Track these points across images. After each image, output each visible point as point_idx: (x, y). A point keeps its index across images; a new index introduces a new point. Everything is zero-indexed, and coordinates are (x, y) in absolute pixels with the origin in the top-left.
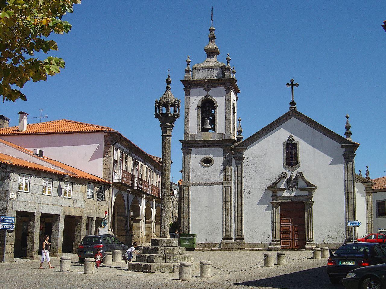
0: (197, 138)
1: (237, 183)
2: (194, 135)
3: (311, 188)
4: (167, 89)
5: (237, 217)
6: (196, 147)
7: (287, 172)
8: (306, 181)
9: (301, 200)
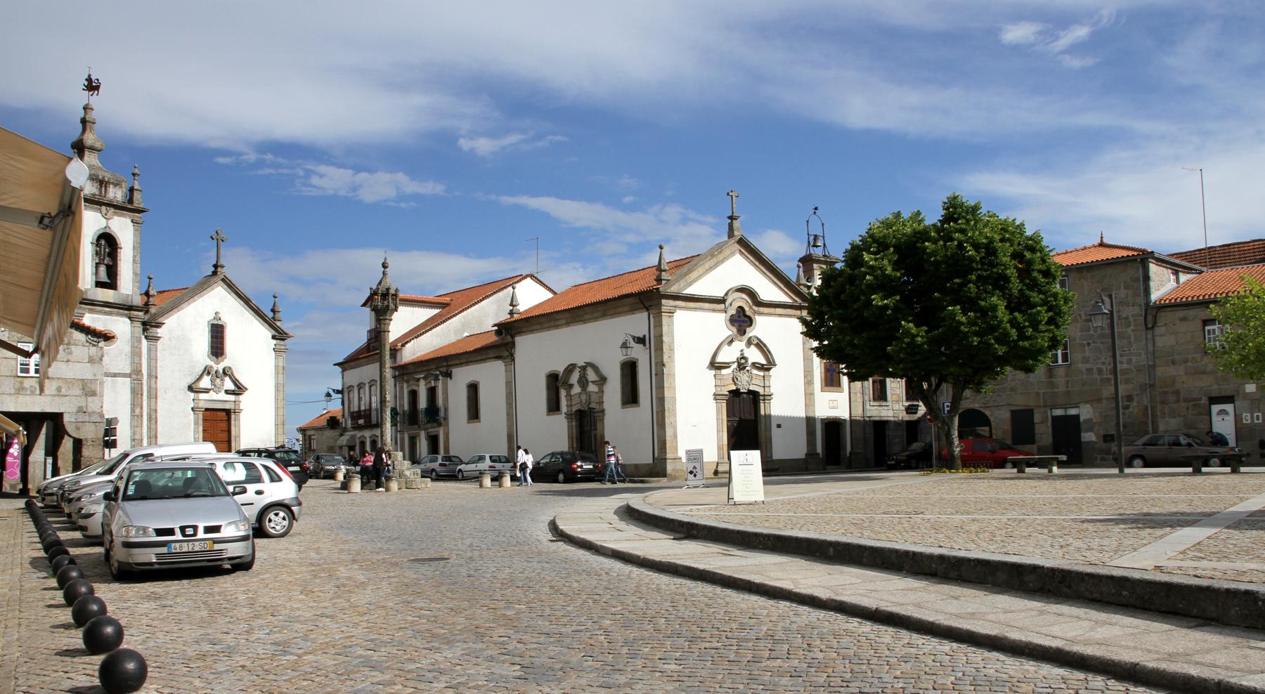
0: (90, 296)
1: (150, 376)
2: (87, 290)
3: (239, 389)
4: (384, 273)
5: (149, 428)
6: (91, 311)
7: (212, 363)
8: (235, 382)
9: (227, 406)
